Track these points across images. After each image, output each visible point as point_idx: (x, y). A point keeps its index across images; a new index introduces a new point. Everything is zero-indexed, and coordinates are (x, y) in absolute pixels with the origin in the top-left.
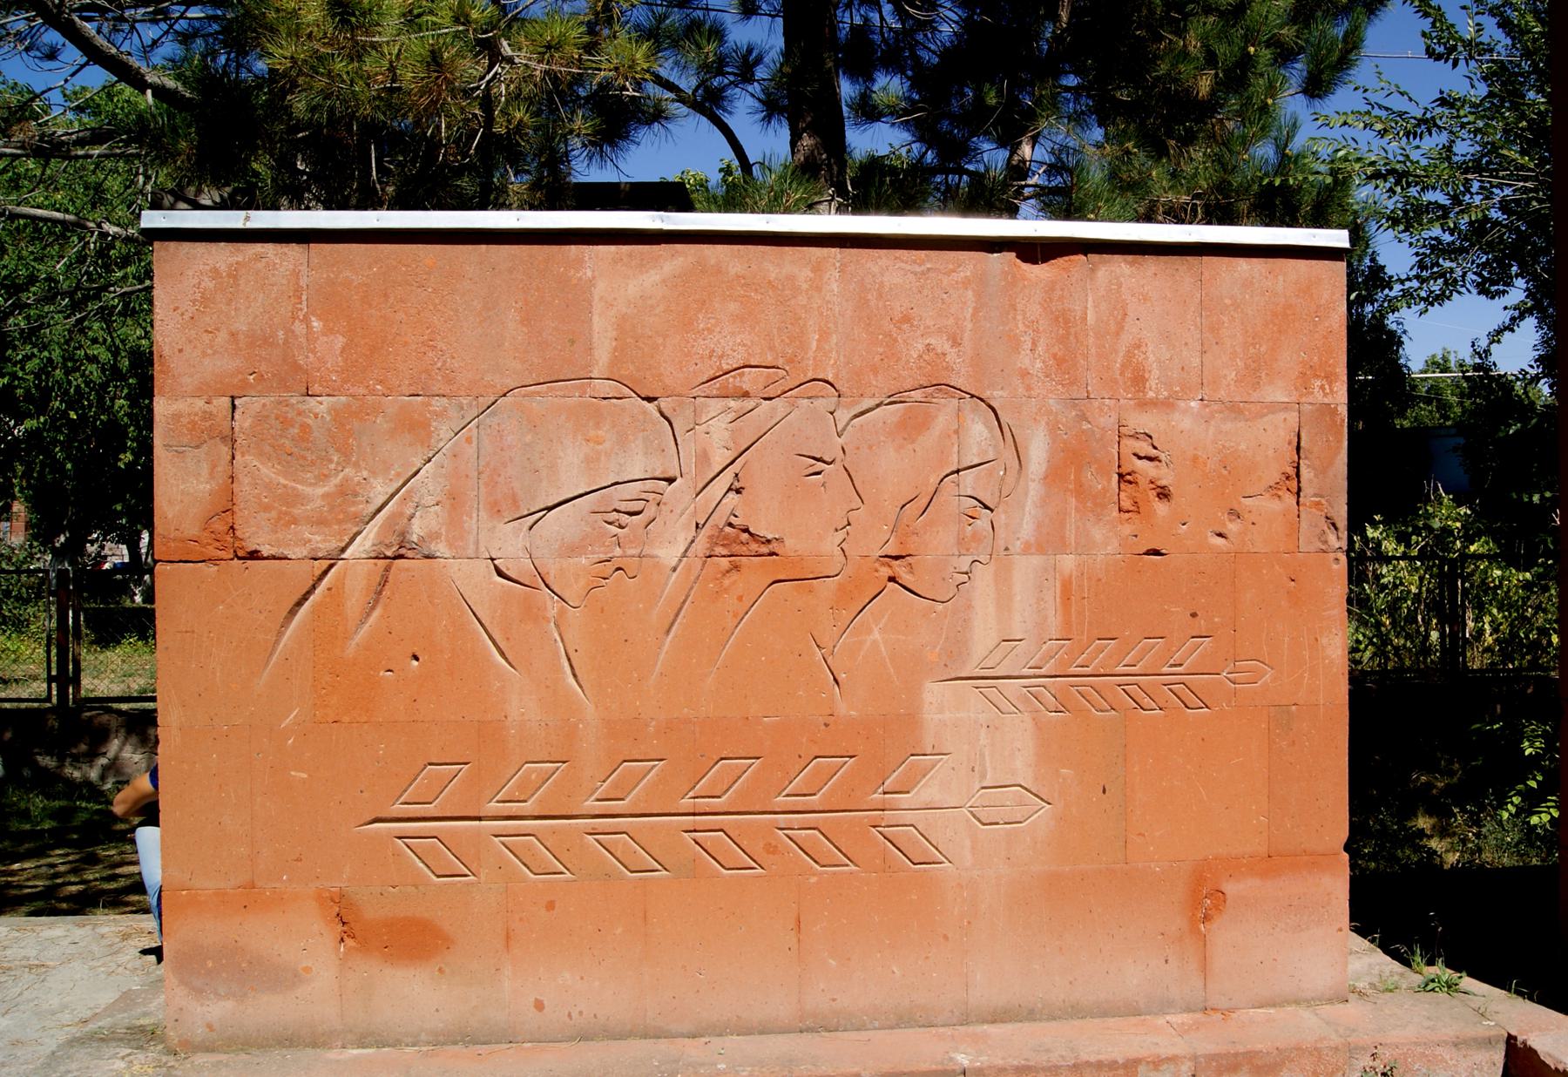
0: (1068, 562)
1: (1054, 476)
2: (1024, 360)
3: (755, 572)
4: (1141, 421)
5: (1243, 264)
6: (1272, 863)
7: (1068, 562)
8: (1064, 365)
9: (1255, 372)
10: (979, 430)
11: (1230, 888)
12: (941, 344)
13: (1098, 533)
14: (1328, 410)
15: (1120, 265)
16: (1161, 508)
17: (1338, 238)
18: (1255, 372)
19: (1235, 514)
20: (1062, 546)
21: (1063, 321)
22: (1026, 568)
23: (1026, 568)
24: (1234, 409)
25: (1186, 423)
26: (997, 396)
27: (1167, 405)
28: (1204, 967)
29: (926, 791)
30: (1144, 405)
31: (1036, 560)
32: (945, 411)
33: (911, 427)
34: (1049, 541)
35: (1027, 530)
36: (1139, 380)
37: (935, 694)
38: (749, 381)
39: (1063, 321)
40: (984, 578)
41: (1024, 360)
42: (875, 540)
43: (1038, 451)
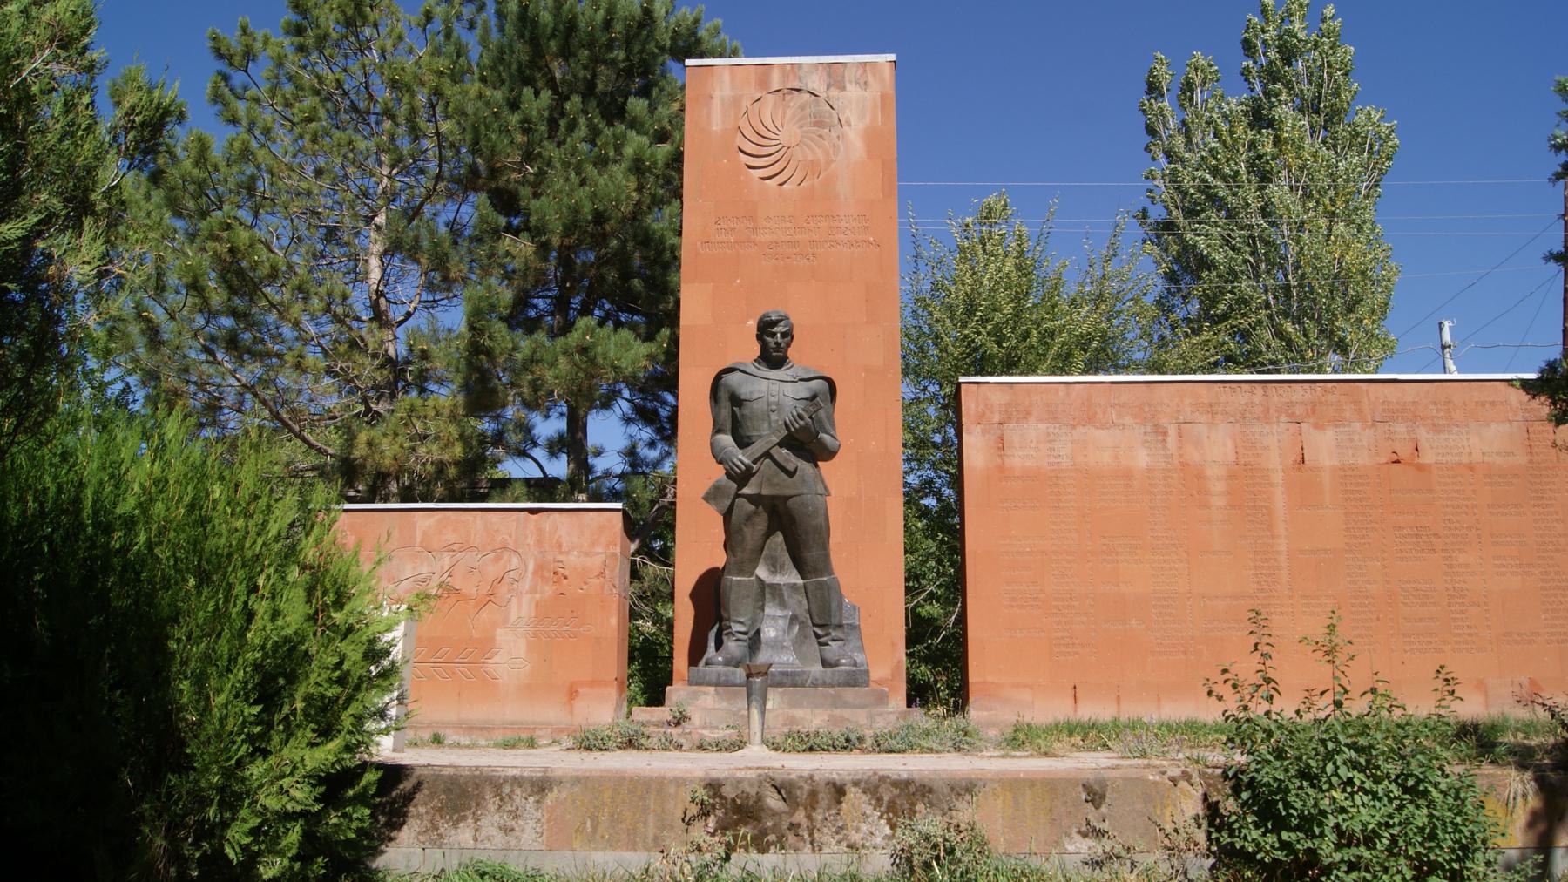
0: (538, 596)
1: (535, 573)
2: (528, 541)
3: (454, 598)
4: (560, 558)
5: (591, 513)
6: (593, 683)
7: (538, 596)
8: (539, 542)
9: (593, 544)
10: (515, 561)
11: (580, 690)
12: (507, 537)
13: (547, 588)
14: (614, 554)
15: (556, 515)
16: (565, 582)
17: (619, 505)
18: (593, 544)
19: (585, 583)
20: (536, 592)
21: (540, 531)
22: (526, 598)
23: (526, 598)
24: (587, 554)
25: (573, 558)
26: (520, 551)
27: (567, 553)
28: (571, 713)
29: (496, 659)
30: (561, 553)
31: (529, 596)
32: (506, 555)
33: (498, 559)
34: (533, 591)
35: (527, 587)
36: (560, 546)
37: (500, 633)
38: (455, 547)
39: (540, 531)
40: (514, 600)
41: (528, 541)
42: (485, 590)
43: (531, 567)
